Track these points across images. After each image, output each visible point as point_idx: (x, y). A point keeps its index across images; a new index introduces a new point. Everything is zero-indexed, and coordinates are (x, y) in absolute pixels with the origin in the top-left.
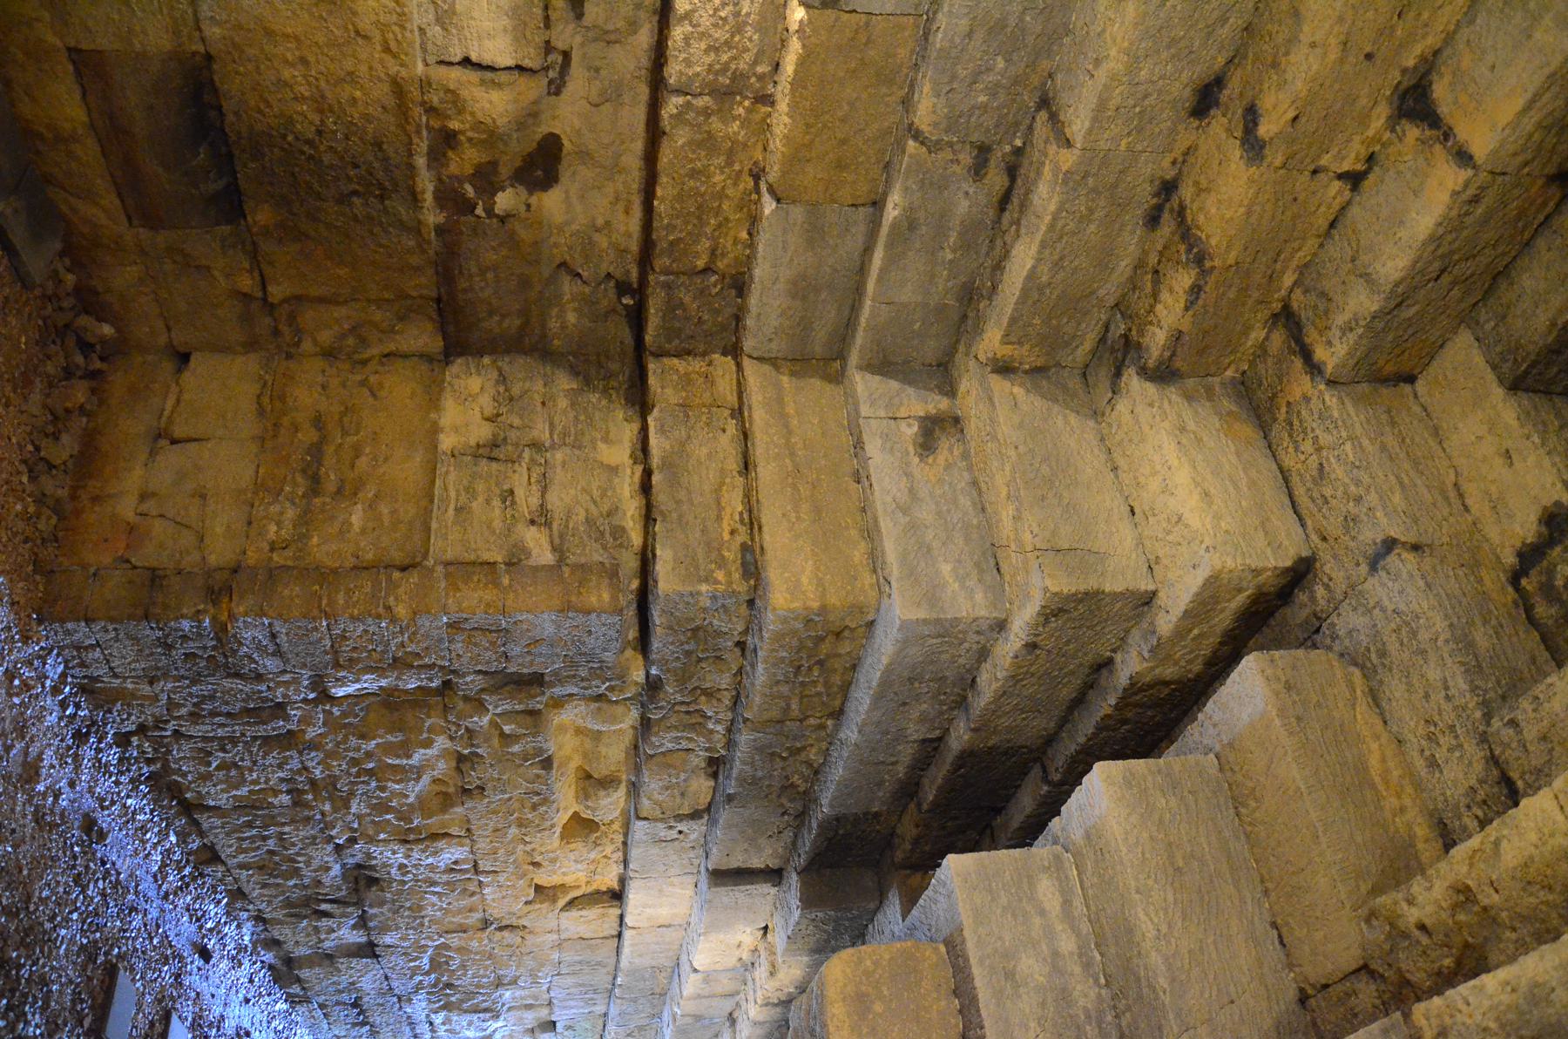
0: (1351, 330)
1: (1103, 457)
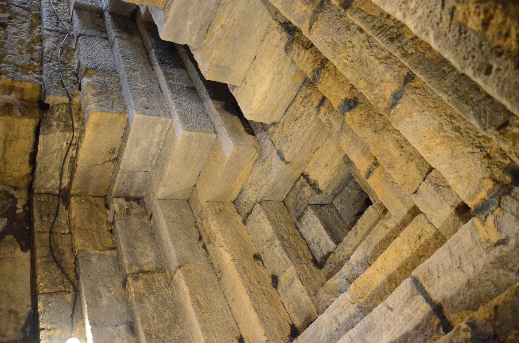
1: (263, 34)
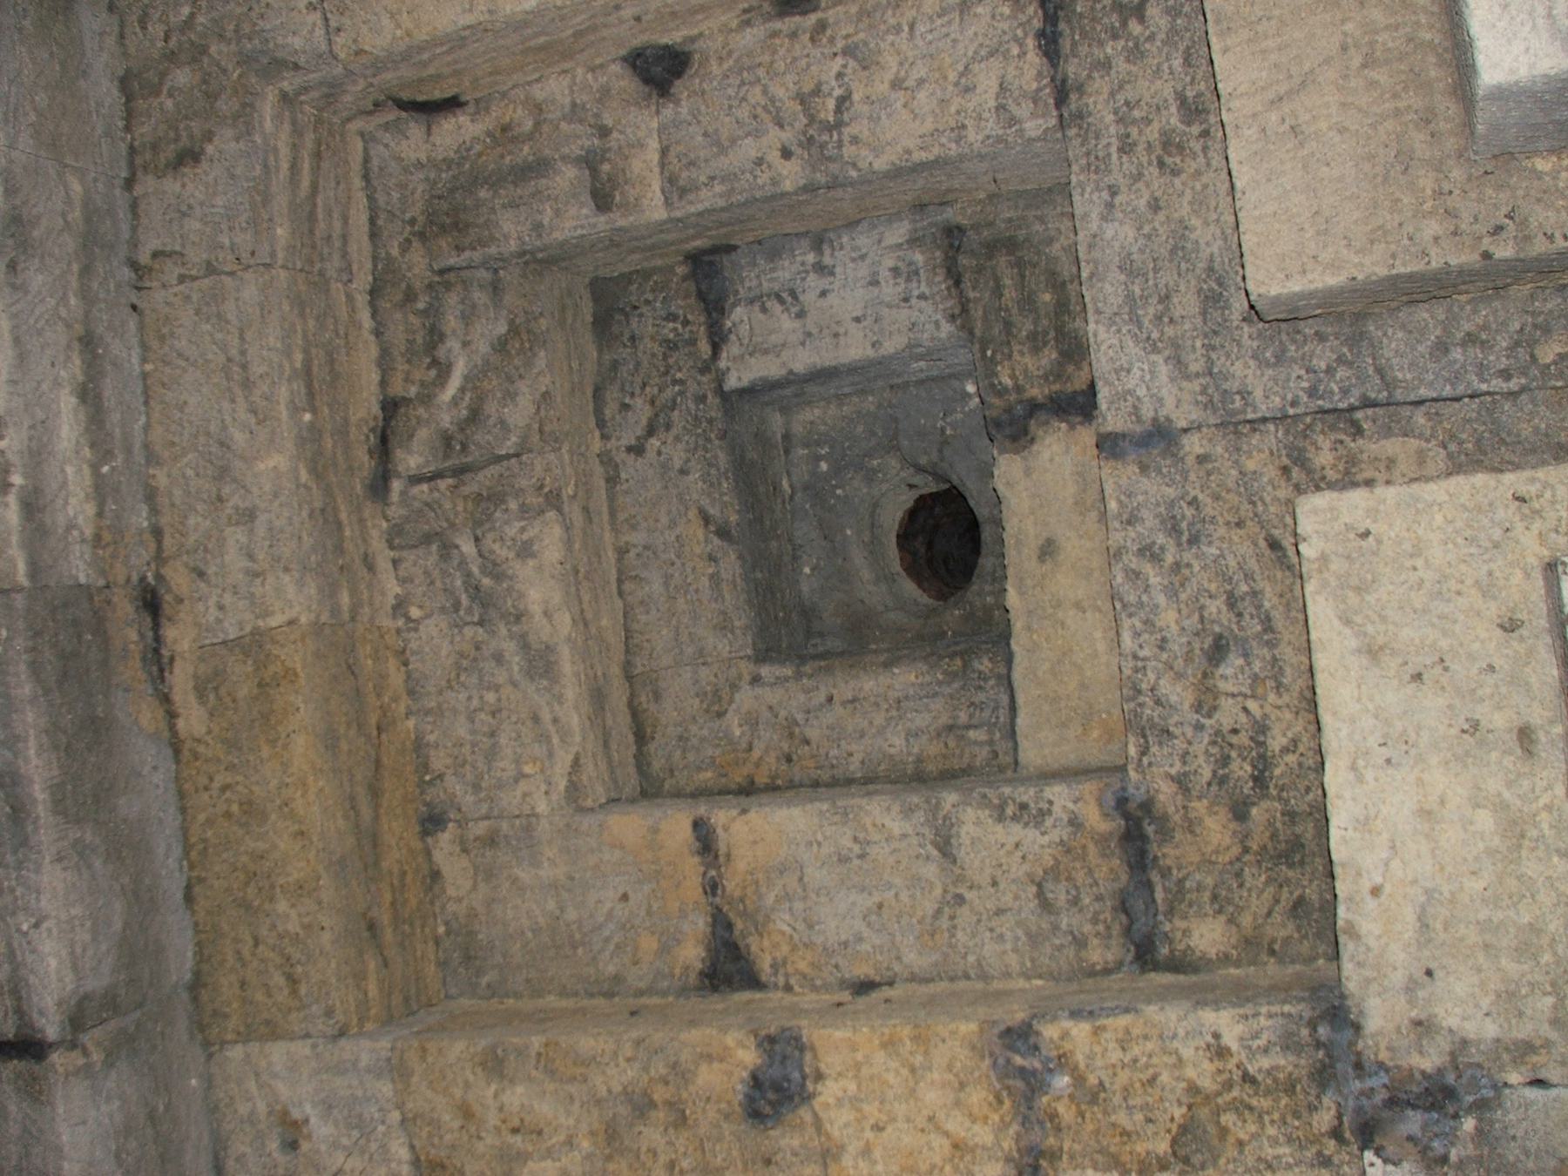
0: (1023, 807)
